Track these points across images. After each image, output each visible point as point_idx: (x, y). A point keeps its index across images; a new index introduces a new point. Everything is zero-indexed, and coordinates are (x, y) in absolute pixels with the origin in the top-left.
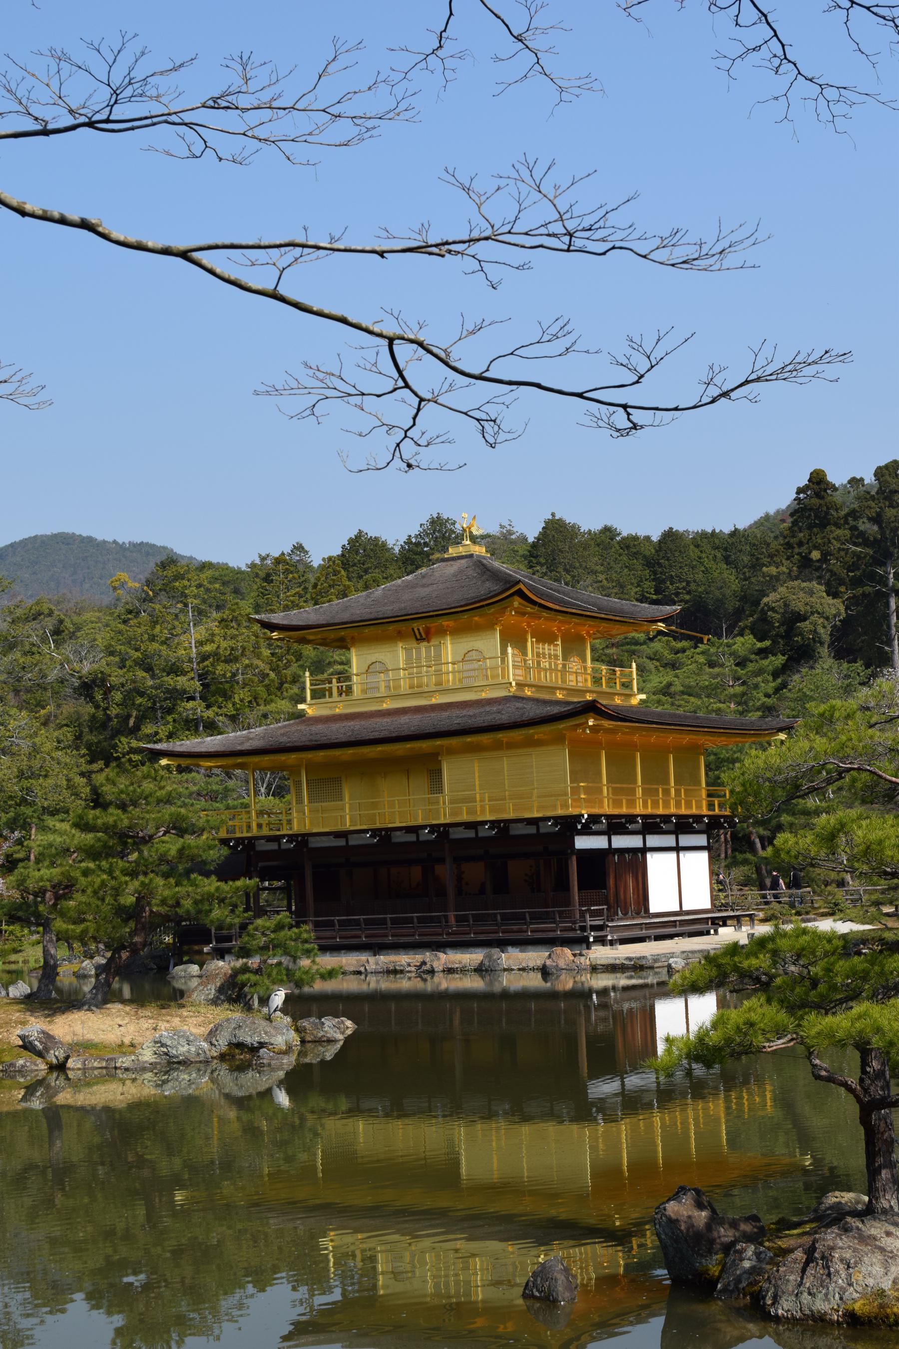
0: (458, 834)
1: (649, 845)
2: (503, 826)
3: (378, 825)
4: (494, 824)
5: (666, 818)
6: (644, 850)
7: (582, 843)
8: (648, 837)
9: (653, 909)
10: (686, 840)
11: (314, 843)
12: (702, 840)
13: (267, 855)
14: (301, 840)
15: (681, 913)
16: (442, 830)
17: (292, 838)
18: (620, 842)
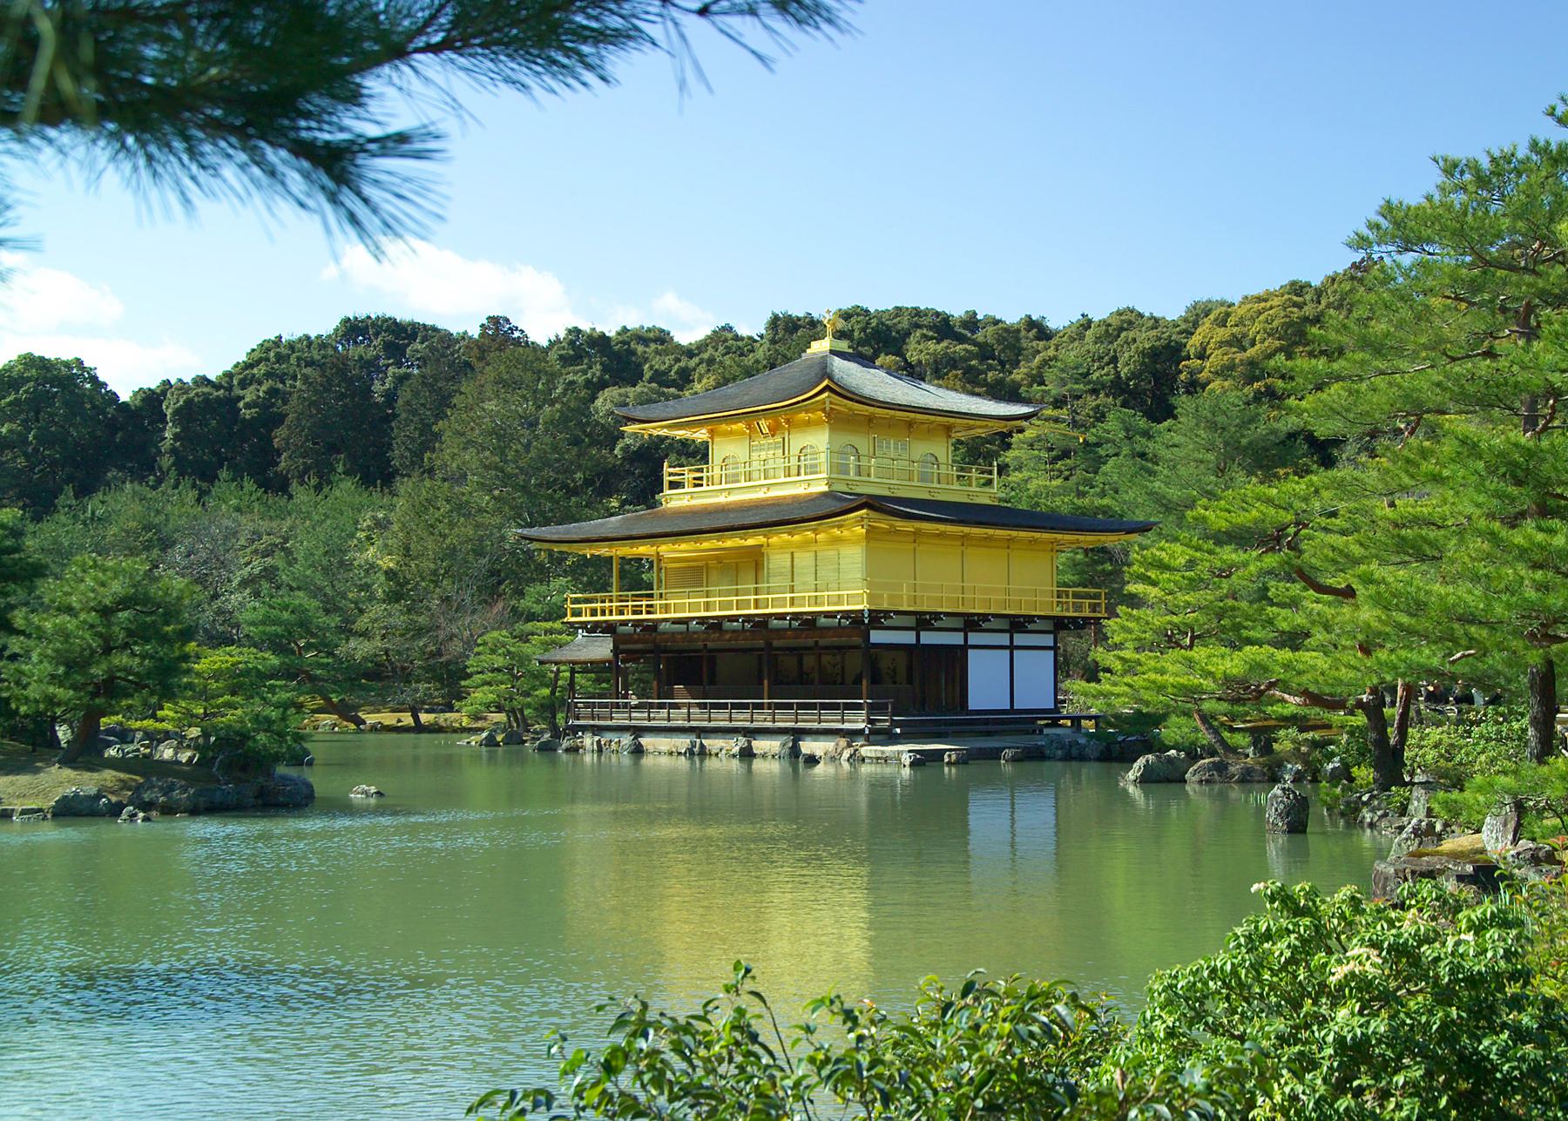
0: (775, 623)
1: (970, 642)
2: (808, 622)
3: (703, 614)
4: (796, 616)
5: (985, 617)
6: (965, 647)
7: (877, 637)
8: (970, 635)
9: (973, 704)
10: (1020, 639)
11: (662, 626)
12: (1048, 640)
13: (628, 638)
14: (652, 628)
15: (1012, 710)
16: (760, 624)
17: (636, 623)
18: (928, 638)
